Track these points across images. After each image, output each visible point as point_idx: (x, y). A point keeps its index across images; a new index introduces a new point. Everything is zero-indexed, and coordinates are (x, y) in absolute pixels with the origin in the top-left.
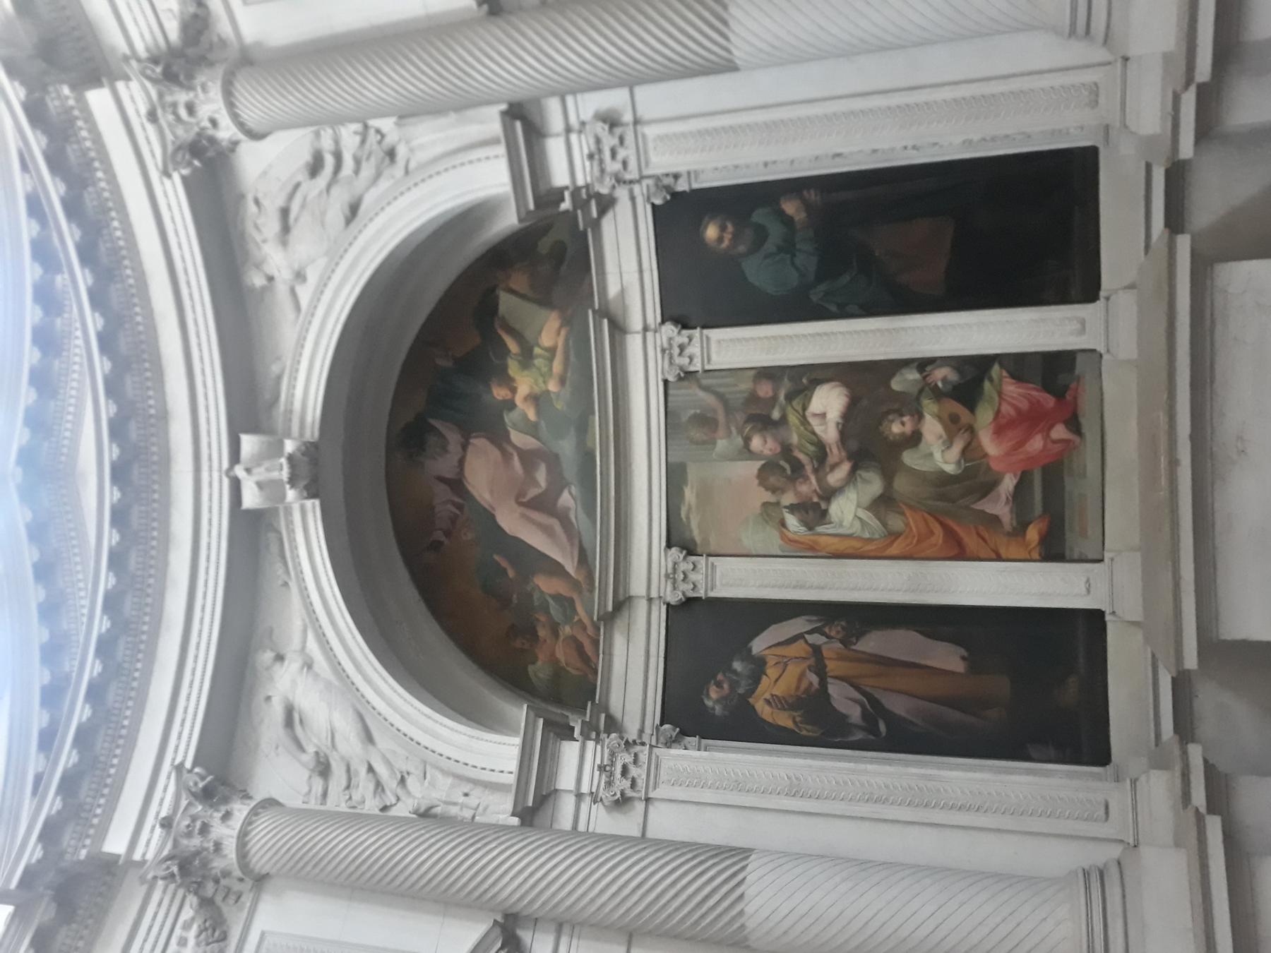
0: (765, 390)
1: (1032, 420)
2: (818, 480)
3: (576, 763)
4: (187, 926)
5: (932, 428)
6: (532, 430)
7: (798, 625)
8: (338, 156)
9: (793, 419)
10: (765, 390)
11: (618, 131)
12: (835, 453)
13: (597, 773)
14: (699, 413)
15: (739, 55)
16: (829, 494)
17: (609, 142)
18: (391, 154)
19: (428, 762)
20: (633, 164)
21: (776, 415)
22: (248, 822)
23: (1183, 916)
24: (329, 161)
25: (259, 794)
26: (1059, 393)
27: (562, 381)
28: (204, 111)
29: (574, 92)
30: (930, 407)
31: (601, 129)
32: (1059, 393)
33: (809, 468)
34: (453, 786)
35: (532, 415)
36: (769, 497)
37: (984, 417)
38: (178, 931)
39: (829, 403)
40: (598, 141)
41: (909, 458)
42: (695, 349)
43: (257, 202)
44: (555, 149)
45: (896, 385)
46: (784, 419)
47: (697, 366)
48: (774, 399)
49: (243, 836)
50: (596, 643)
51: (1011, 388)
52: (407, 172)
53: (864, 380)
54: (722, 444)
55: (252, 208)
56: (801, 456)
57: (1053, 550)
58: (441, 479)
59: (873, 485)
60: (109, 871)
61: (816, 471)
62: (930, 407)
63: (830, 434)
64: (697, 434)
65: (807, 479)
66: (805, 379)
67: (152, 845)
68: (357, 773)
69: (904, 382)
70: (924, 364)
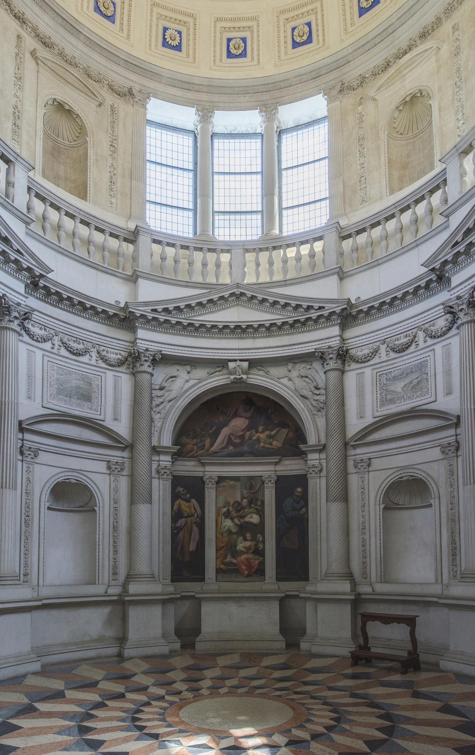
0: (259, 503)
2: (235, 516)
3: (166, 460)
4: (120, 354)
8: (319, 395)
9: (251, 510)
10: (259, 503)
11: (319, 472)
12: (242, 520)
13: (164, 465)
14: (253, 485)
15: (329, 504)
16: (232, 519)
17: (317, 470)
18: (319, 411)
19: (164, 419)
20: (311, 475)
21: (252, 506)
22: (148, 373)
23: (150, 591)
24: (318, 392)
25: (155, 373)
29: (326, 462)
31: (319, 468)
33: (239, 514)
34: (159, 427)
36: (231, 503)
38: (119, 351)
39: (255, 519)
40: (317, 467)
43: (310, 369)
44: (316, 456)
46: (251, 508)
48: (257, 505)
49: (145, 372)
50: (192, 457)
52: (314, 415)
55: (308, 367)
56: (242, 512)
57: (218, 571)
58: (237, 410)
59: (234, 530)
60: (133, 330)
61: (238, 516)
63: (247, 519)
65: (236, 513)
67: (142, 345)
68: (161, 398)
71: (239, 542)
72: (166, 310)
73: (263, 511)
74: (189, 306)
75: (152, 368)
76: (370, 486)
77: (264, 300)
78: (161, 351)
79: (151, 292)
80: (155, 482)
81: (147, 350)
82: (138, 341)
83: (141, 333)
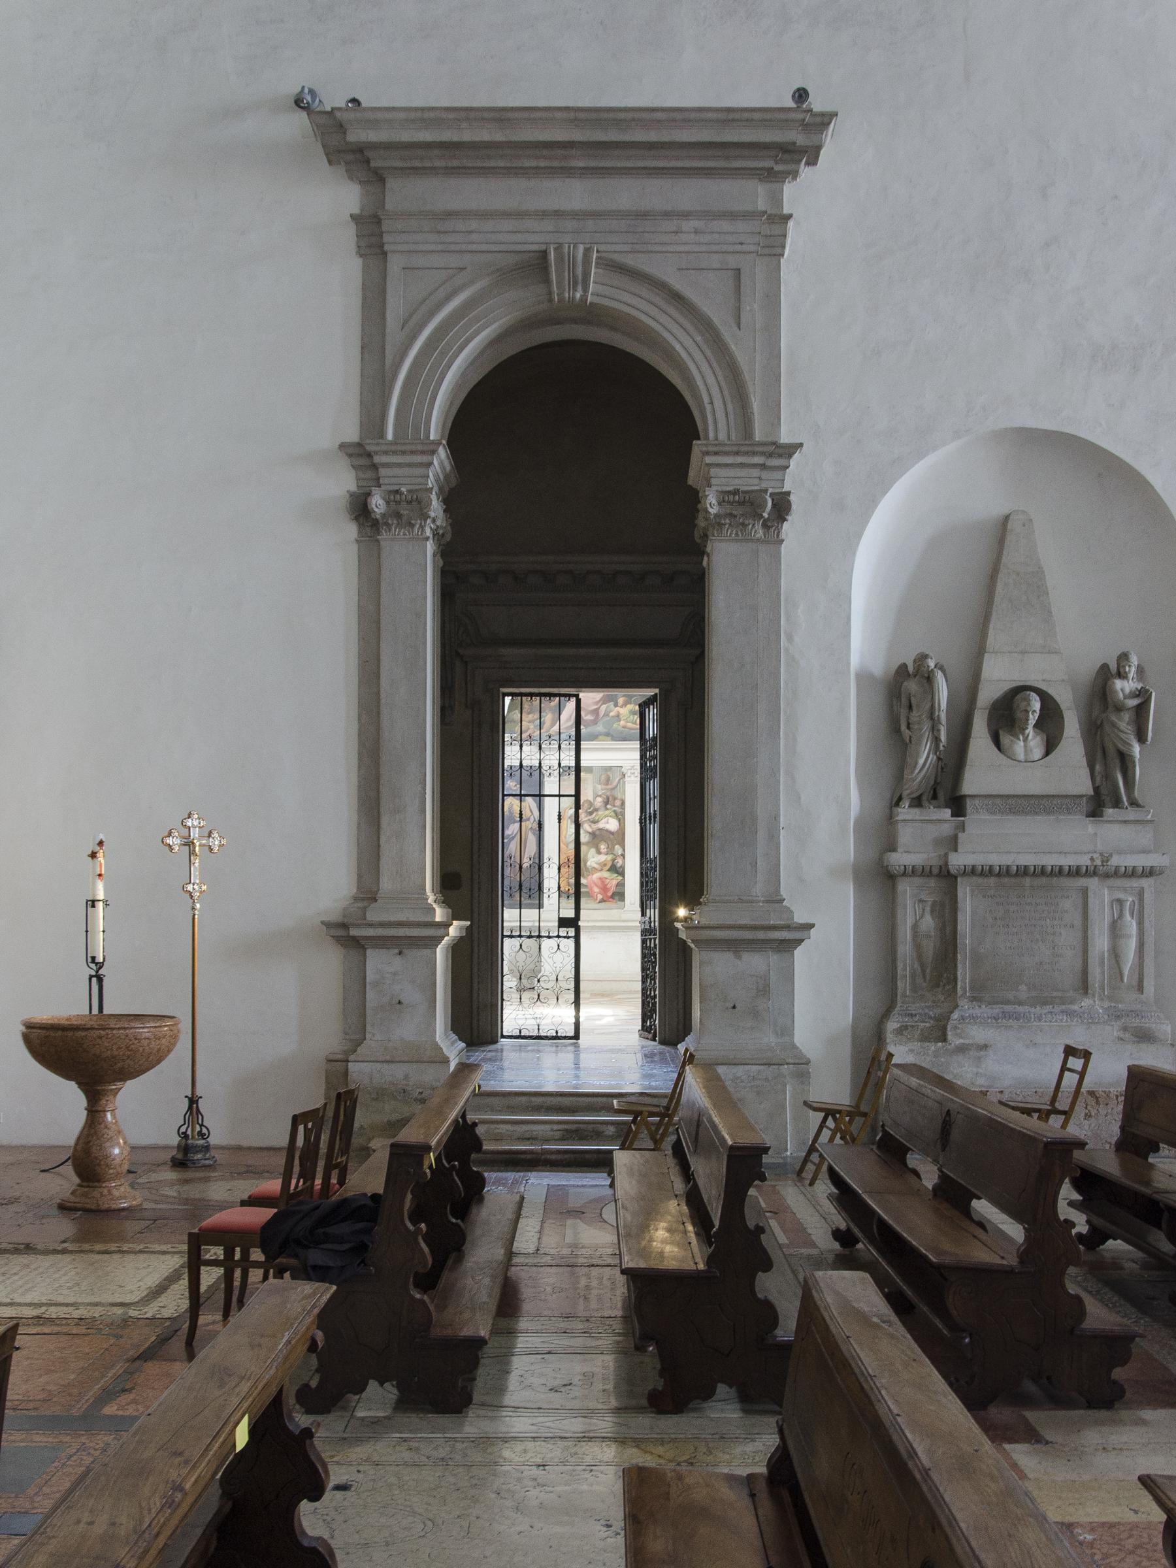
0: (618, 803)
1: (604, 889)
5: (602, 858)
6: (606, 714)
7: (536, 813)
9: (607, 812)
12: (595, 826)
26: (612, 897)
27: (624, 727)
30: (610, 857)
32: (612, 897)
35: (612, 714)
37: (606, 874)
39: (612, 825)
41: (593, 850)
42: (633, 778)
45: (617, 847)
47: (627, 779)
51: (614, 882)
53: (619, 837)
54: (599, 787)
62: (610, 857)
63: (601, 825)
64: (603, 777)
66: (620, 816)
69: (618, 850)
70: (623, 856)
71: (590, 855)
73: (623, 814)
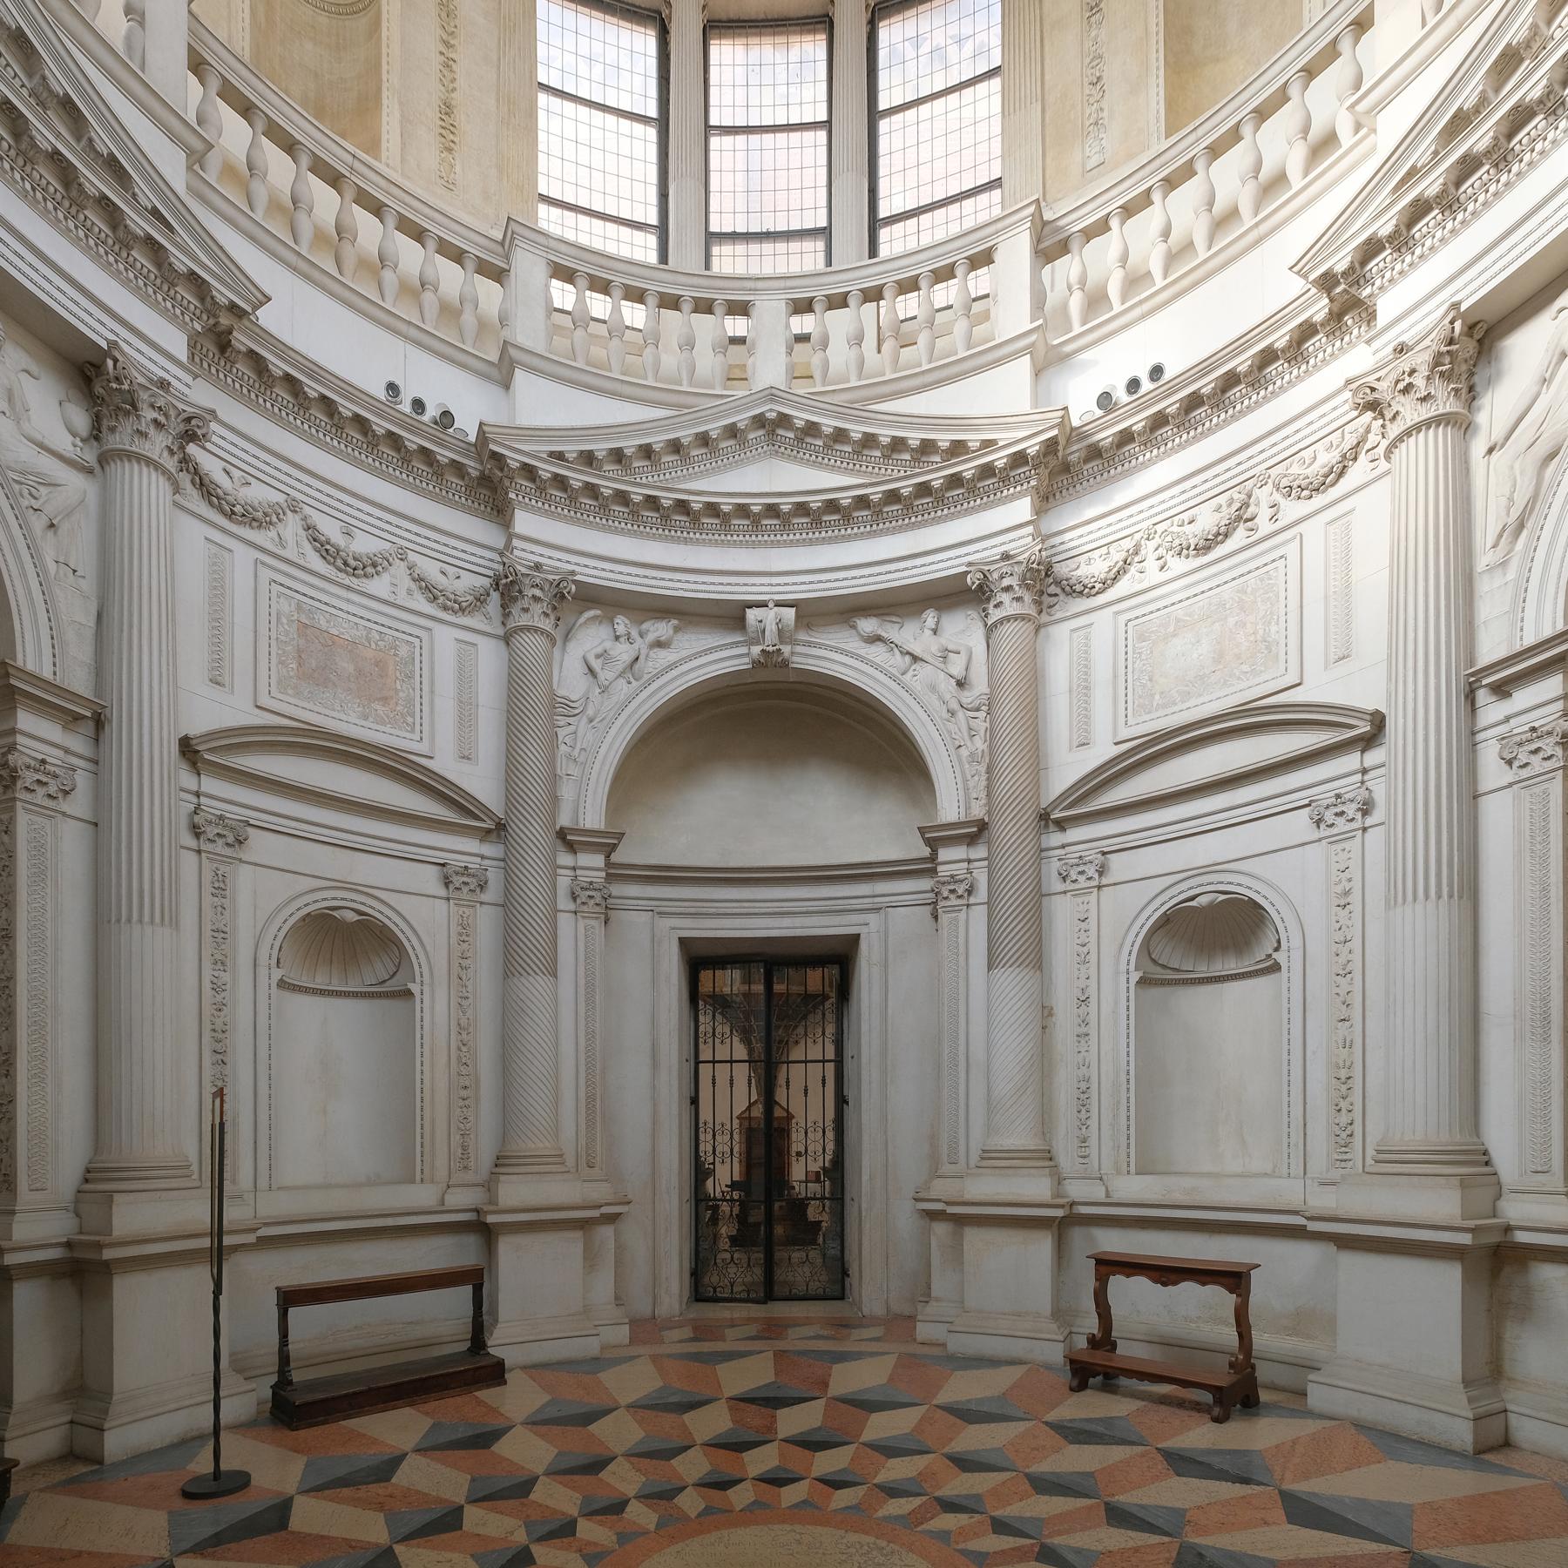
28: (1005, 598)
49: (536, 630)
67: (524, 555)
72: (588, 458)
74: (647, 452)
75: (552, 617)
76: (1104, 920)
77: (840, 435)
78: (573, 573)
79: (544, 409)
80: (565, 921)
81: (538, 567)
82: (515, 542)
83: (524, 522)
